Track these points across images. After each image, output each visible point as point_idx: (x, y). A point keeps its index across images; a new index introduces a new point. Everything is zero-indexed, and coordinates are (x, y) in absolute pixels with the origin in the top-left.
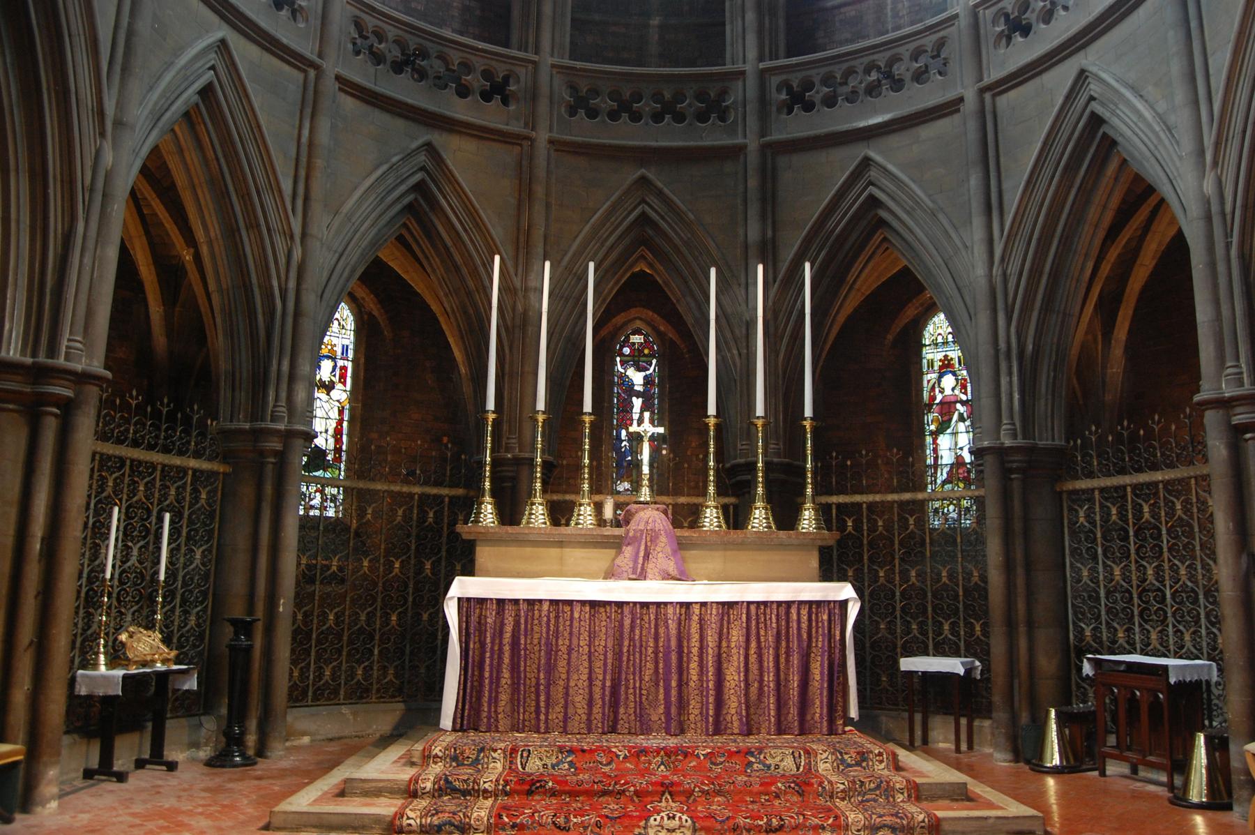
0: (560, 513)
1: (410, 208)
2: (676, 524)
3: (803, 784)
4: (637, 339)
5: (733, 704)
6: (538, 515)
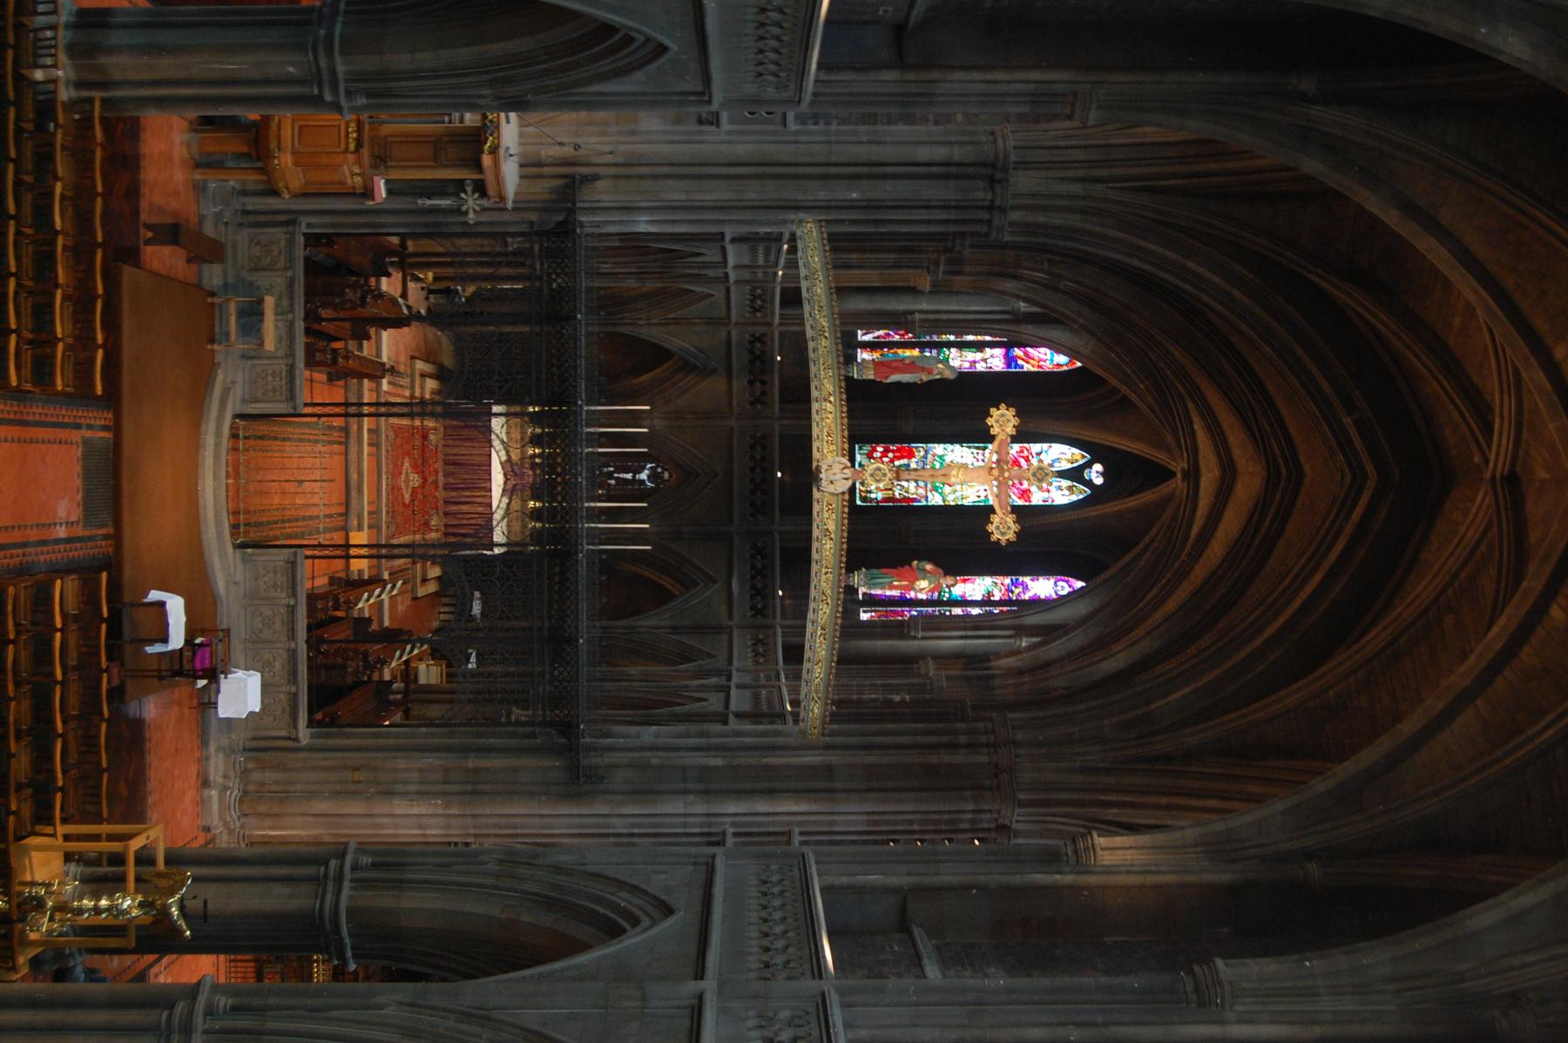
0: (536, 441)
1: (687, 362)
3: (427, 524)
4: (666, 475)
5: (454, 508)
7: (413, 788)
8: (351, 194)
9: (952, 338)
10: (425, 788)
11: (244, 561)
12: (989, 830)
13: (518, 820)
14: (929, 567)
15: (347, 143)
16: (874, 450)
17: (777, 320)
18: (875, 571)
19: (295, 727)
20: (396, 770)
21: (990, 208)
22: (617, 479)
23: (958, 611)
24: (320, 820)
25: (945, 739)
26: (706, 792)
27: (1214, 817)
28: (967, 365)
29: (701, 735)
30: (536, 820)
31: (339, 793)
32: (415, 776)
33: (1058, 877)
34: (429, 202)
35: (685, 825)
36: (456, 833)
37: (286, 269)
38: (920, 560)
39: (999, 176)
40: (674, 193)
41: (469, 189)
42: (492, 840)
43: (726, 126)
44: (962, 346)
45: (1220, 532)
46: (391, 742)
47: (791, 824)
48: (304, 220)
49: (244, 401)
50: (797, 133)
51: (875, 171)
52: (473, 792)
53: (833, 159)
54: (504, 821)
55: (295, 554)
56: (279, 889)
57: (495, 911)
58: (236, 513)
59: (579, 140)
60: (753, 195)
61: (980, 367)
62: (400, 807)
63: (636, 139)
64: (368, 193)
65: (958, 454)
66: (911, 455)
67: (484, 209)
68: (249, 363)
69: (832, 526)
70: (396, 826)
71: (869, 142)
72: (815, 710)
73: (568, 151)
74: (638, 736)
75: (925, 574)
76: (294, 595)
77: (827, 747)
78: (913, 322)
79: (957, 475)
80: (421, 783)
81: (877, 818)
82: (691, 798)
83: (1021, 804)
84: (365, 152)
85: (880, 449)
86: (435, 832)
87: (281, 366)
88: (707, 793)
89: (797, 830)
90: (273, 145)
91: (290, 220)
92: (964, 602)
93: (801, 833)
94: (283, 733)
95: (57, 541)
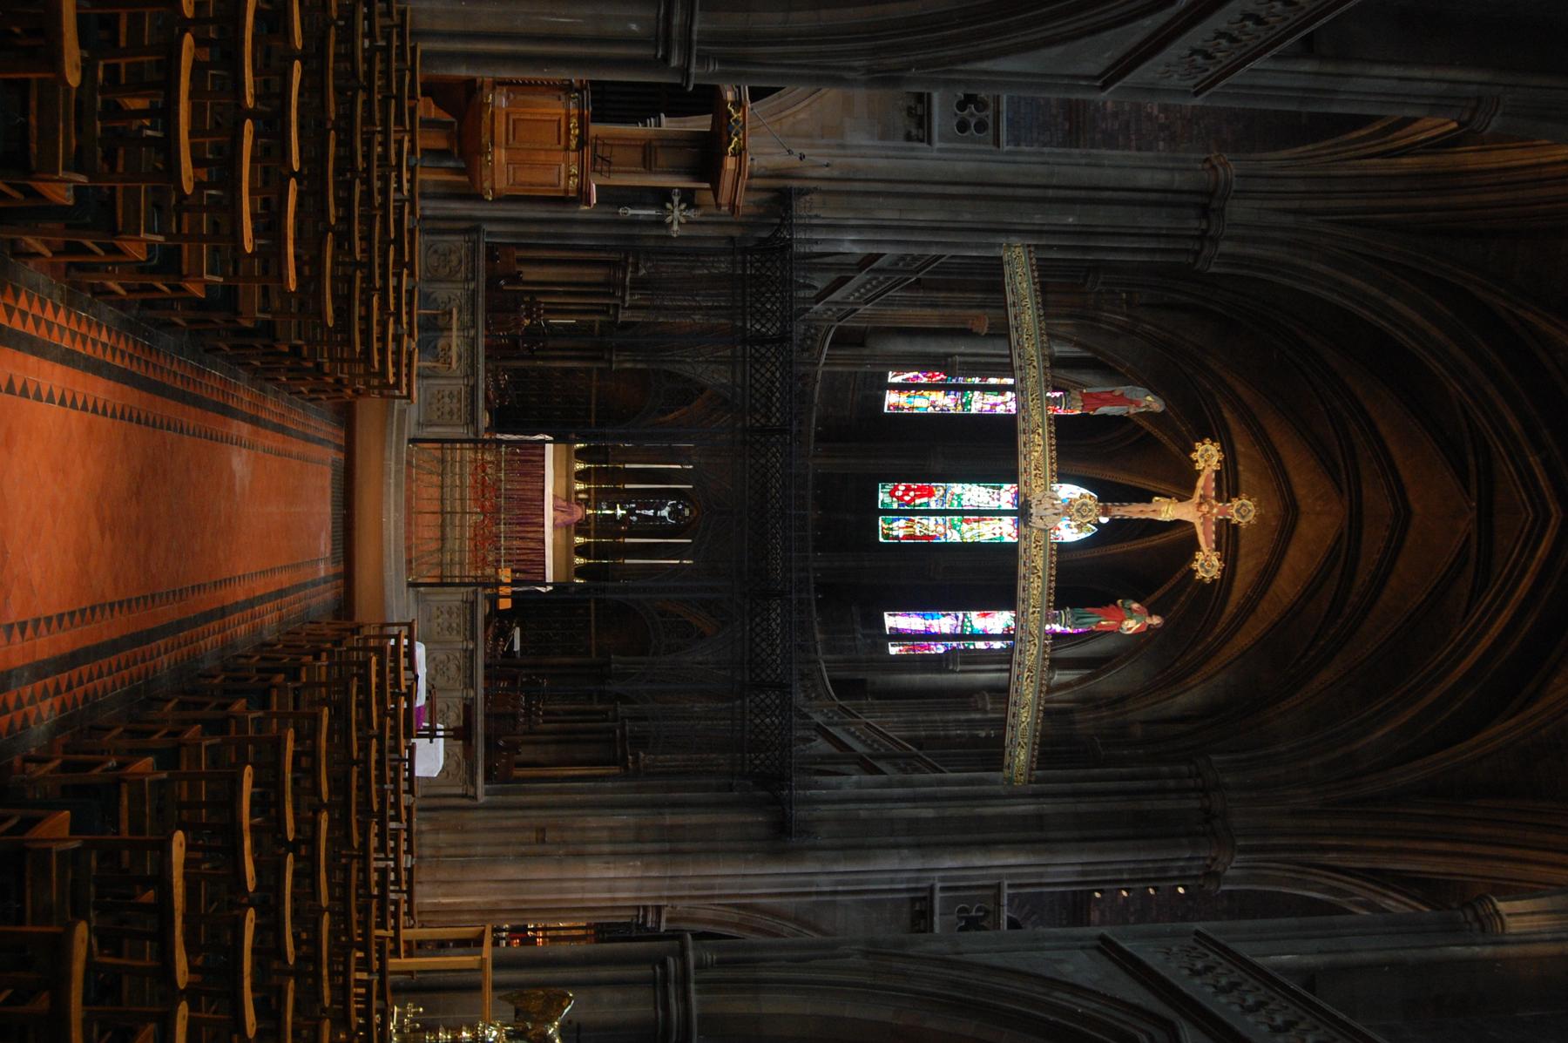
0: (582, 476)
2: (578, 524)
4: (687, 512)
6: (580, 466)
7: (607, 848)
8: (563, 200)
9: (977, 380)
10: (619, 848)
11: (419, 599)
12: (1196, 877)
13: (719, 881)
14: (1135, 606)
15: (568, 140)
16: (896, 489)
17: (823, 360)
18: (1080, 610)
19: (473, 783)
20: (583, 829)
21: (1202, 237)
22: (639, 516)
23: (981, 645)
24: (504, 886)
25: (1152, 784)
26: (919, 846)
27: (1439, 859)
28: (988, 407)
29: (903, 784)
30: (739, 880)
31: (524, 855)
32: (605, 834)
33: (1477, 949)
34: (631, 212)
35: (892, 881)
36: (648, 896)
37: (467, 280)
38: (1125, 598)
39: (1215, 204)
40: (888, 213)
41: (676, 199)
42: (686, 903)
43: (937, 144)
44: (985, 389)
45: (1285, 567)
46: (578, 798)
47: (999, 876)
48: (487, 227)
49: (419, 424)
50: (1009, 153)
51: (1088, 196)
52: (672, 852)
53: (1054, 181)
54: (705, 881)
55: (475, 593)
56: (606, 995)
57: (885, 1014)
58: (409, 548)
59: (805, 152)
60: (967, 217)
61: (1000, 410)
62: (596, 870)
63: (849, 152)
64: (582, 196)
65: (974, 494)
66: (931, 494)
67: (690, 222)
68: (425, 382)
69: (1039, 563)
70: (583, 890)
71: (1087, 165)
72: (1021, 756)
73: (793, 161)
74: (838, 787)
75: (1131, 614)
76: (473, 637)
77: (1036, 795)
78: (953, 365)
79: (972, 513)
80: (611, 842)
81: (1090, 868)
82: (906, 852)
83: (1243, 850)
84: (588, 150)
85: (902, 488)
86: (624, 895)
87: (459, 385)
88: (921, 847)
89: (1006, 882)
90: (485, 138)
91: (473, 228)
92: (986, 637)
93: (1010, 886)
94: (459, 791)
95: (315, 584)
